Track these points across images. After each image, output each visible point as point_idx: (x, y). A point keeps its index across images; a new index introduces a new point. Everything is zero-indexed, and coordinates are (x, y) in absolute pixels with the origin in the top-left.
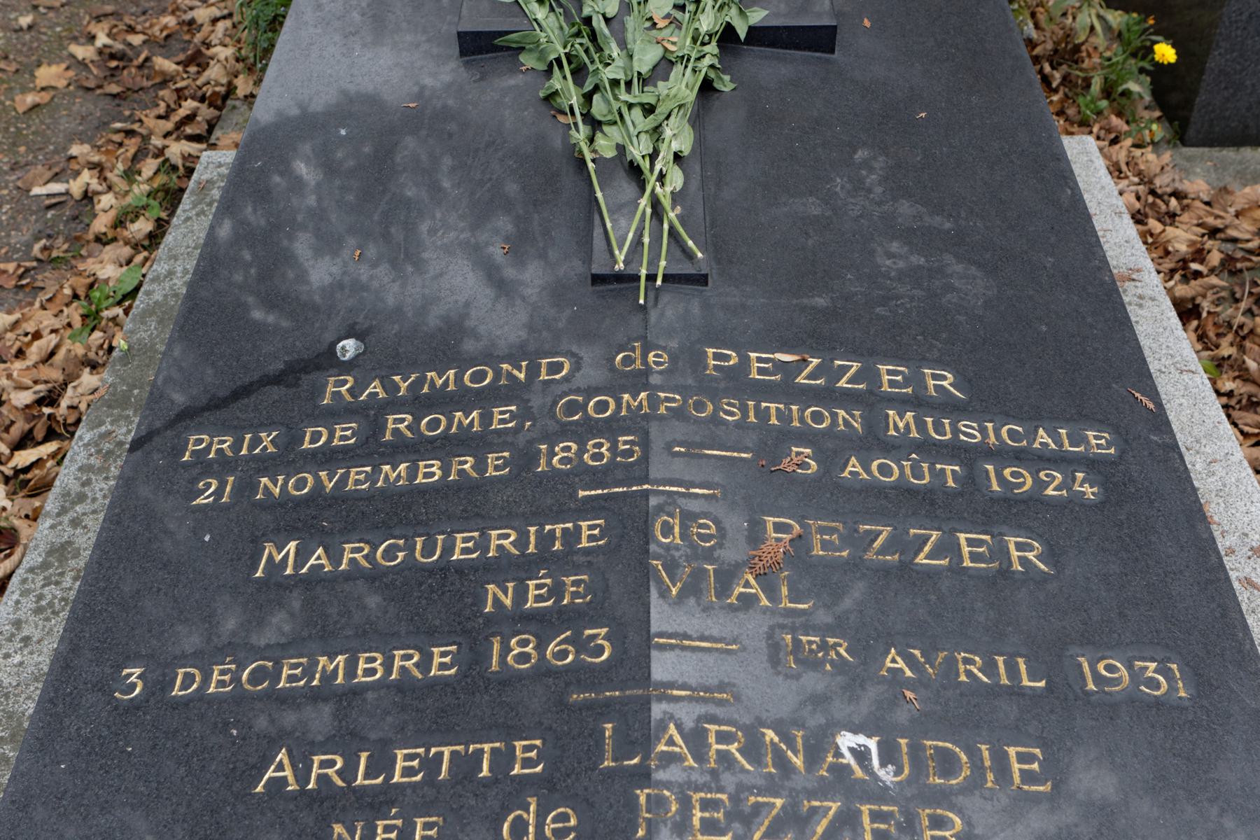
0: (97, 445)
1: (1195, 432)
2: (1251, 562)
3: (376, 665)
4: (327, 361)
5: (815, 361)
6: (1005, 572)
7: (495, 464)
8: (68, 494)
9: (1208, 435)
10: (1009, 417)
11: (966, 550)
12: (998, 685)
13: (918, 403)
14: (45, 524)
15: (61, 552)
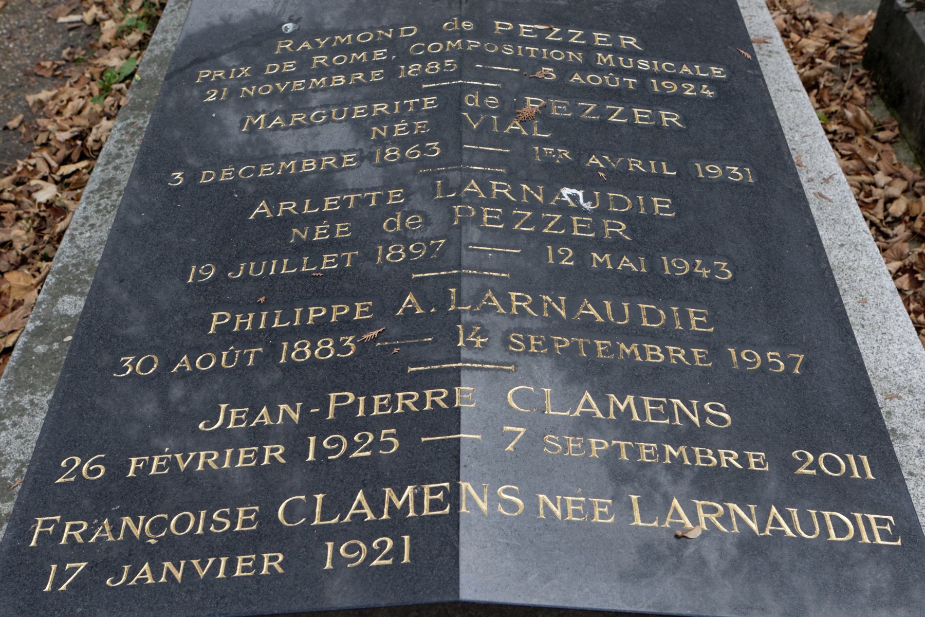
0: (125, 129)
1: (797, 121)
2: (823, 186)
3: (312, 164)
4: (277, 33)
5: (557, 30)
6: (659, 126)
7: (376, 75)
8: (111, 154)
9: (804, 123)
10: (666, 59)
11: (638, 116)
12: (650, 172)
13: (616, 50)
14: (83, 203)
15: (109, 183)
